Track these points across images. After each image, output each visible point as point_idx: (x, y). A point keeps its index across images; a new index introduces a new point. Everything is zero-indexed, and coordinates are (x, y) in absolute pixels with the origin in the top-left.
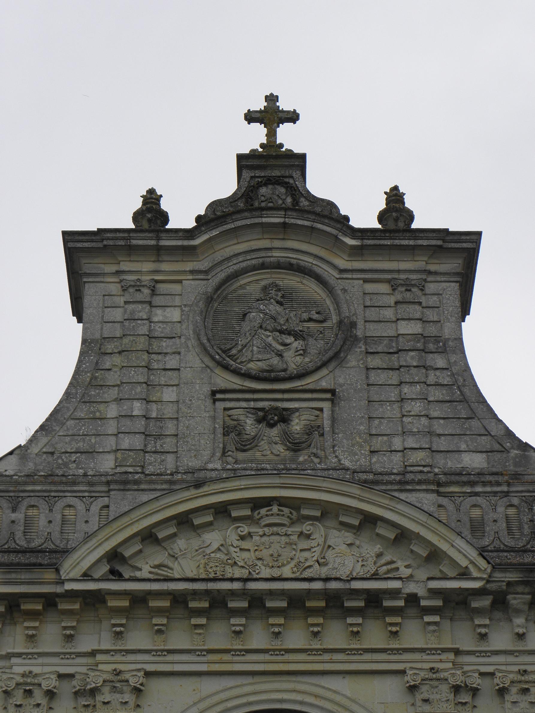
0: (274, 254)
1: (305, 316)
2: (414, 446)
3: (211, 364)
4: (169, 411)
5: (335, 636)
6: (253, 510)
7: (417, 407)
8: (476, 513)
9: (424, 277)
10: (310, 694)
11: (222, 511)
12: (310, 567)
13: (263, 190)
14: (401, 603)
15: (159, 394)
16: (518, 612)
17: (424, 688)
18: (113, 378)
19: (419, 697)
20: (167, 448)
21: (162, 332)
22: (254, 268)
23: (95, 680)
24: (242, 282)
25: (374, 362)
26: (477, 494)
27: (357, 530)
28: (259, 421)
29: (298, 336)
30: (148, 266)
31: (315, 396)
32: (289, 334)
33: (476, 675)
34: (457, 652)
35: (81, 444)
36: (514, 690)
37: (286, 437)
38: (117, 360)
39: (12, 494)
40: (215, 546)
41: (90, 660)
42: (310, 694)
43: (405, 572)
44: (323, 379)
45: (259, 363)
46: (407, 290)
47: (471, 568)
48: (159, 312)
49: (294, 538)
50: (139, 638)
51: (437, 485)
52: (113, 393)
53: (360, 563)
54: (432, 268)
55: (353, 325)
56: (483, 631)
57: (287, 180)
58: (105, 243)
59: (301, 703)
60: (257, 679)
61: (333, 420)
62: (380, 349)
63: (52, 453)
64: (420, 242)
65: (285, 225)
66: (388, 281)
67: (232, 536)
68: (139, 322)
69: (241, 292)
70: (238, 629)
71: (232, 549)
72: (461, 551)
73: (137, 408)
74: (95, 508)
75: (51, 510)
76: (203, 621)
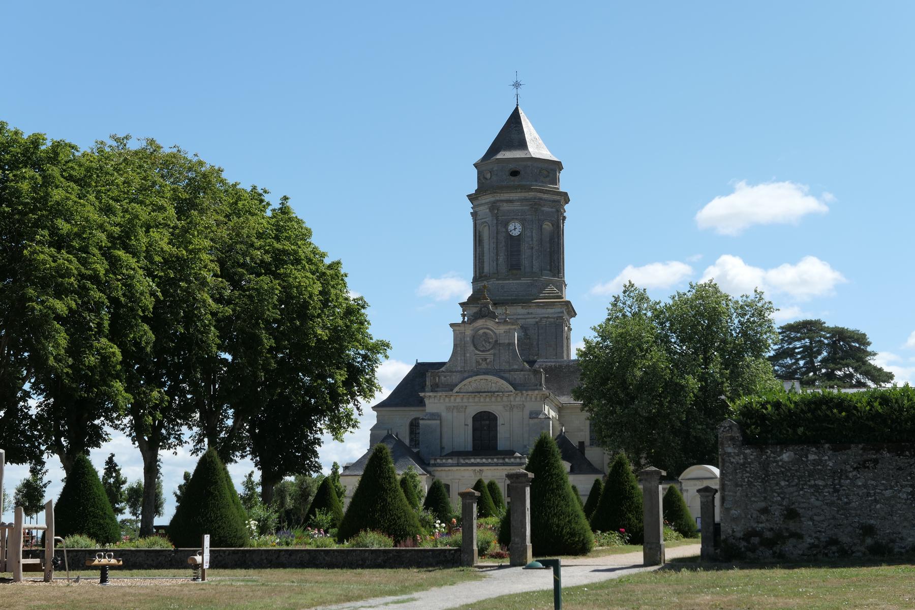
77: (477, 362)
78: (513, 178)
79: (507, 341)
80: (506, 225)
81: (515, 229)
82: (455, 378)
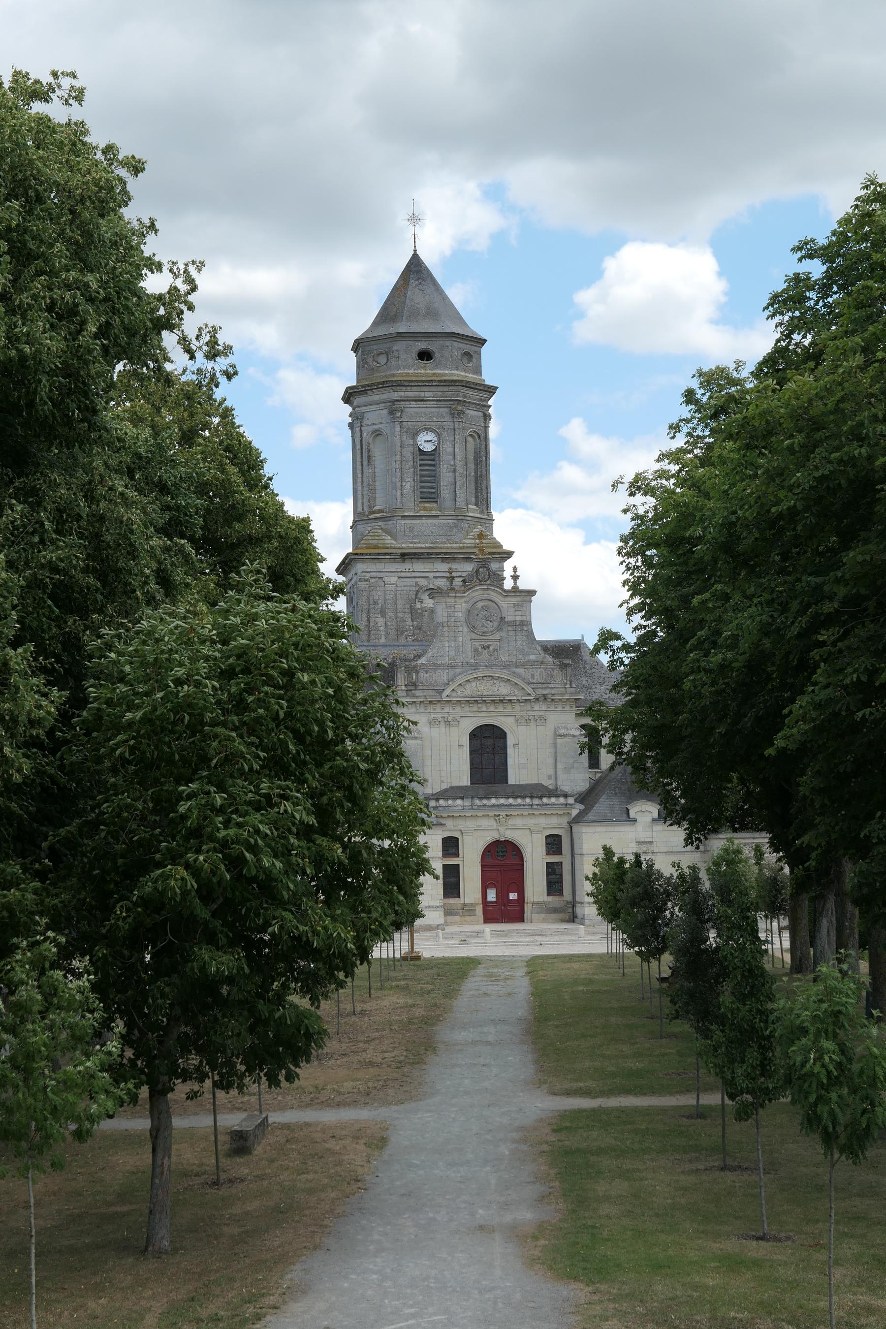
4: (461, 644)
5: (500, 707)
23: (450, 719)
25: (510, 628)
30: (452, 600)
37: (488, 652)
50: (458, 709)
72: (529, 689)
77: (476, 650)
79: (518, 619)
80: (415, 434)
81: (426, 441)
82: (442, 676)
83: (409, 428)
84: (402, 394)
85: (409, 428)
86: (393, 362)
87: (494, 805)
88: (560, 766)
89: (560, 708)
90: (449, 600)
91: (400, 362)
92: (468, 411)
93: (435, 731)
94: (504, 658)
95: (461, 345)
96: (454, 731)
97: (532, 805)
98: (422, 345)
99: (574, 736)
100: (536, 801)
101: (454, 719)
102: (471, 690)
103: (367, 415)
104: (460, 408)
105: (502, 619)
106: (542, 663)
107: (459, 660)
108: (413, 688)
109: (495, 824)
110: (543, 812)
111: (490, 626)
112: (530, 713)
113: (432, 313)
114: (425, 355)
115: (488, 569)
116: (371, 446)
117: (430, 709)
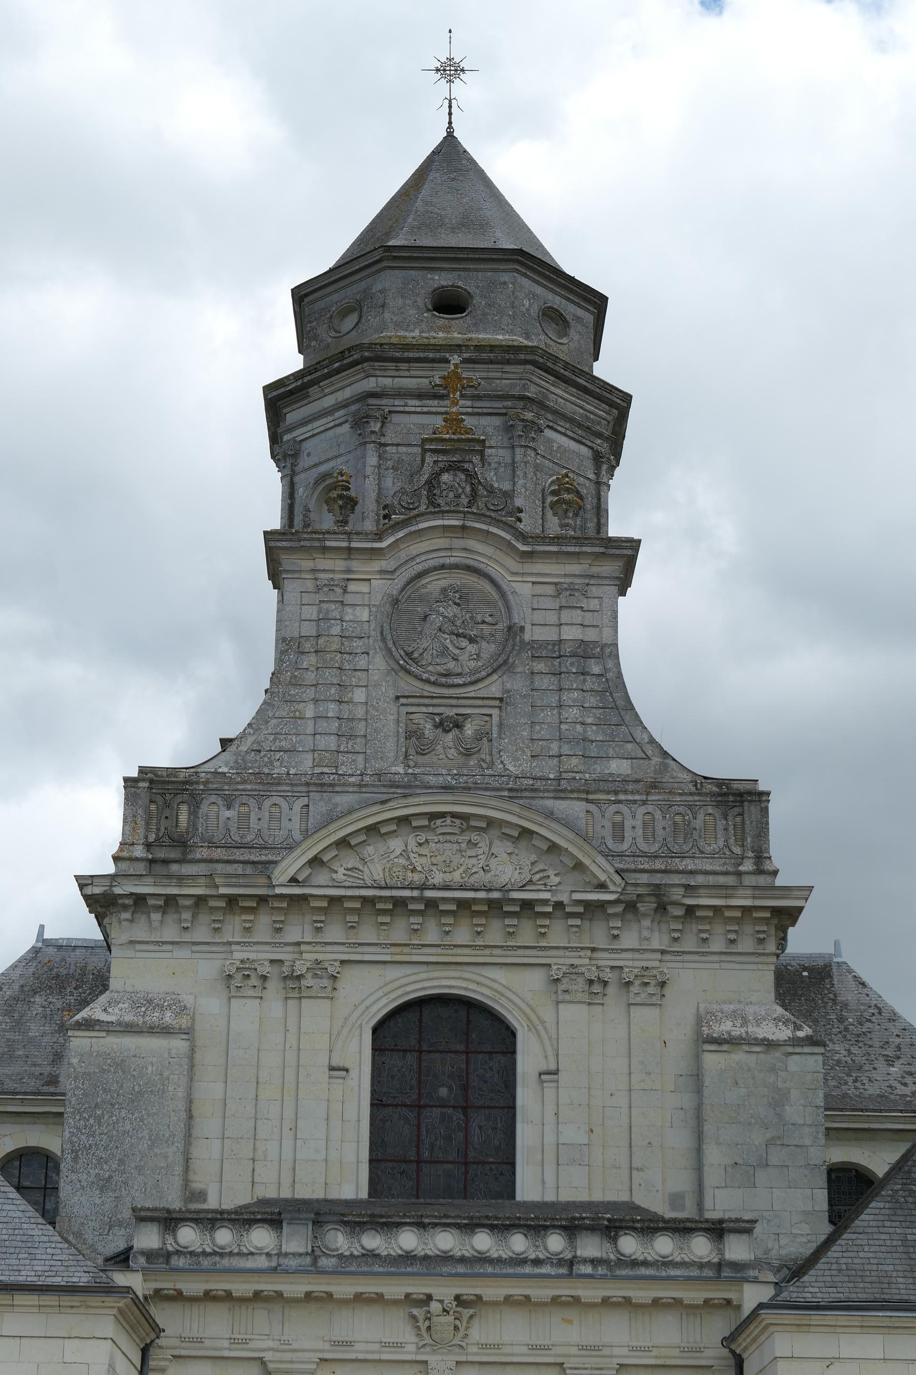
0: (454, 554)
1: (479, 618)
2: (569, 753)
3: (396, 667)
4: (360, 712)
5: (495, 933)
6: (430, 820)
7: (573, 713)
8: (618, 818)
9: (587, 581)
10: (474, 981)
11: (404, 821)
12: (476, 873)
13: (445, 477)
14: (550, 909)
15: (350, 695)
16: (645, 915)
17: (565, 980)
18: (310, 677)
19: (561, 987)
20: (358, 749)
21: (353, 632)
22: (435, 569)
23: (300, 968)
24: (424, 582)
25: (540, 666)
26: (620, 802)
27: (516, 840)
28: (436, 726)
29: (472, 640)
30: (340, 564)
31: (486, 702)
32: (465, 637)
33: (608, 970)
34: (593, 950)
35: (283, 743)
36: (637, 982)
37: (458, 740)
38: (313, 658)
39: (227, 793)
40: (398, 852)
41: (296, 949)
42: (474, 981)
43: (555, 880)
44: (494, 687)
45: (438, 667)
46: (570, 595)
47: (609, 883)
48: (349, 610)
49: (464, 845)
50: (335, 932)
51: (585, 792)
52: (311, 693)
53: (518, 871)
54: (595, 570)
55: (522, 629)
56: (616, 932)
57: (466, 466)
58: (302, 543)
59: (466, 989)
60: (431, 967)
61: (501, 725)
62: (544, 653)
63: (259, 751)
64: (584, 549)
65: (464, 528)
66: (556, 584)
67: (412, 842)
68: (332, 622)
69: (423, 591)
70: (416, 927)
71: (412, 855)
72: (601, 869)
73: (332, 709)
74: (298, 805)
75: (260, 808)
76: (387, 919)
78: (442, 320)
79: (570, 634)
83: (400, 461)
84: (388, 382)
85: (400, 461)
86: (372, 319)
87: (408, 1258)
88: (713, 1156)
89: (718, 944)
90: (323, 563)
91: (387, 315)
92: (548, 433)
93: (246, 1013)
94: (515, 763)
95: (539, 290)
96: (316, 1015)
97: (571, 1263)
98: (442, 279)
99: (769, 1045)
100: (590, 1247)
101: (318, 968)
102: (381, 864)
103: (308, 446)
104: (529, 416)
105: (514, 631)
106: (654, 786)
107: (350, 766)
108: (173, 854)
109: (409, 1336)
110: (617, 1291)
111: (468, 658)
112: (605, 960)
113: (469, 221)
114: (449, 304)
115: (471, 476)
116: (312, 516)
117: (233, 927)
